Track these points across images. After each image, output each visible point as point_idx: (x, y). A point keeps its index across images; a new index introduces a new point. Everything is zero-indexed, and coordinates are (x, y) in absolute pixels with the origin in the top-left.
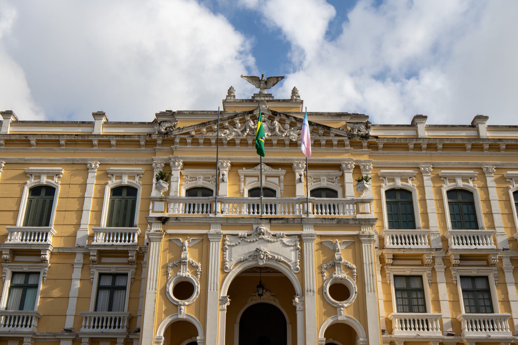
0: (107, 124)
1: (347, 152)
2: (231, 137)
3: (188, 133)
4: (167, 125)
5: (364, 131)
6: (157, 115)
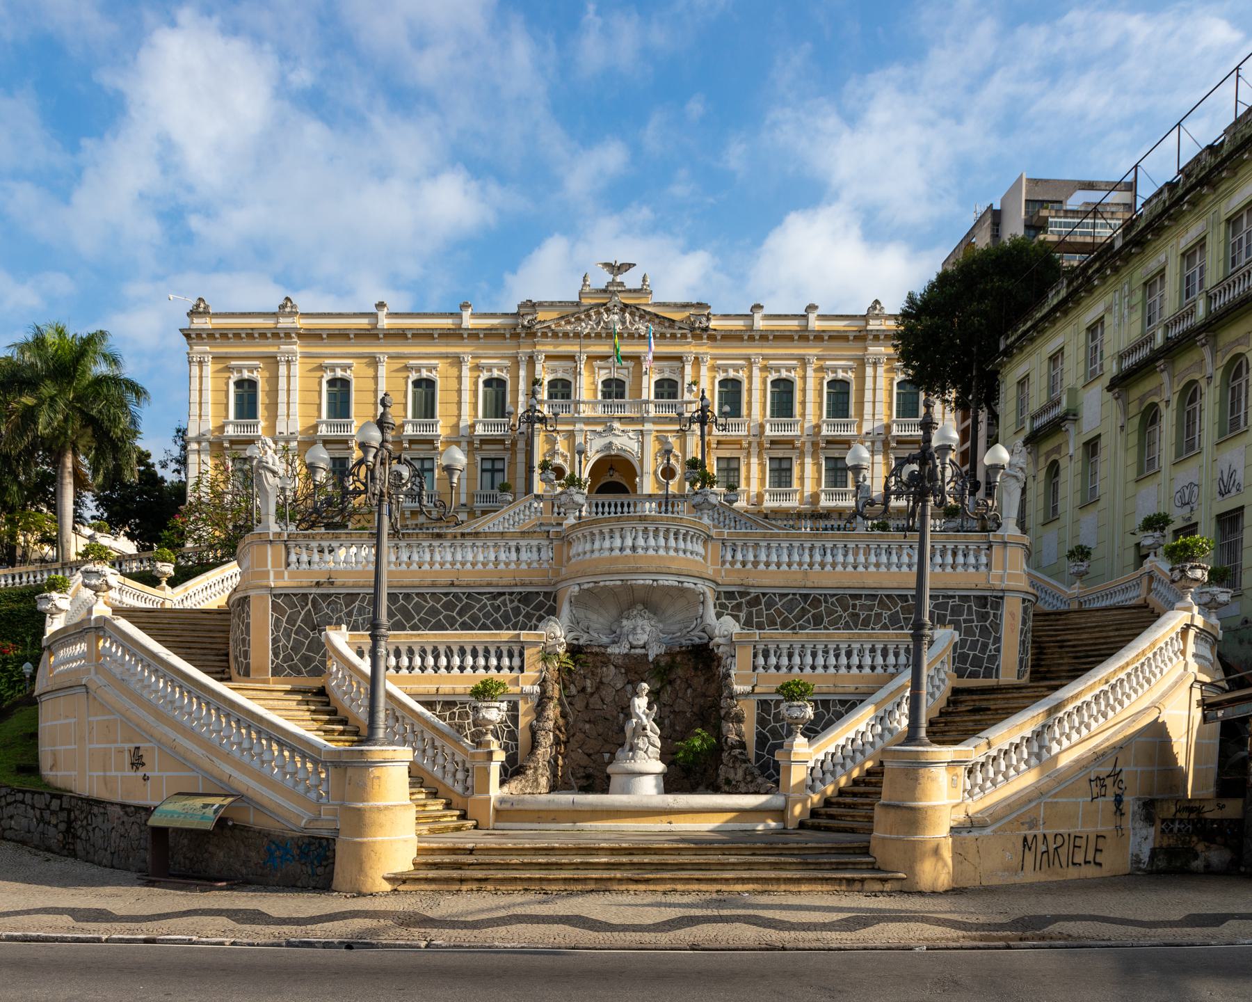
0: (474, 315)
1: (689, 343)
2: (587, 331)
3: (549, 327)
4: (530, 317)
5: (704, 324)
6: (519, 307)
